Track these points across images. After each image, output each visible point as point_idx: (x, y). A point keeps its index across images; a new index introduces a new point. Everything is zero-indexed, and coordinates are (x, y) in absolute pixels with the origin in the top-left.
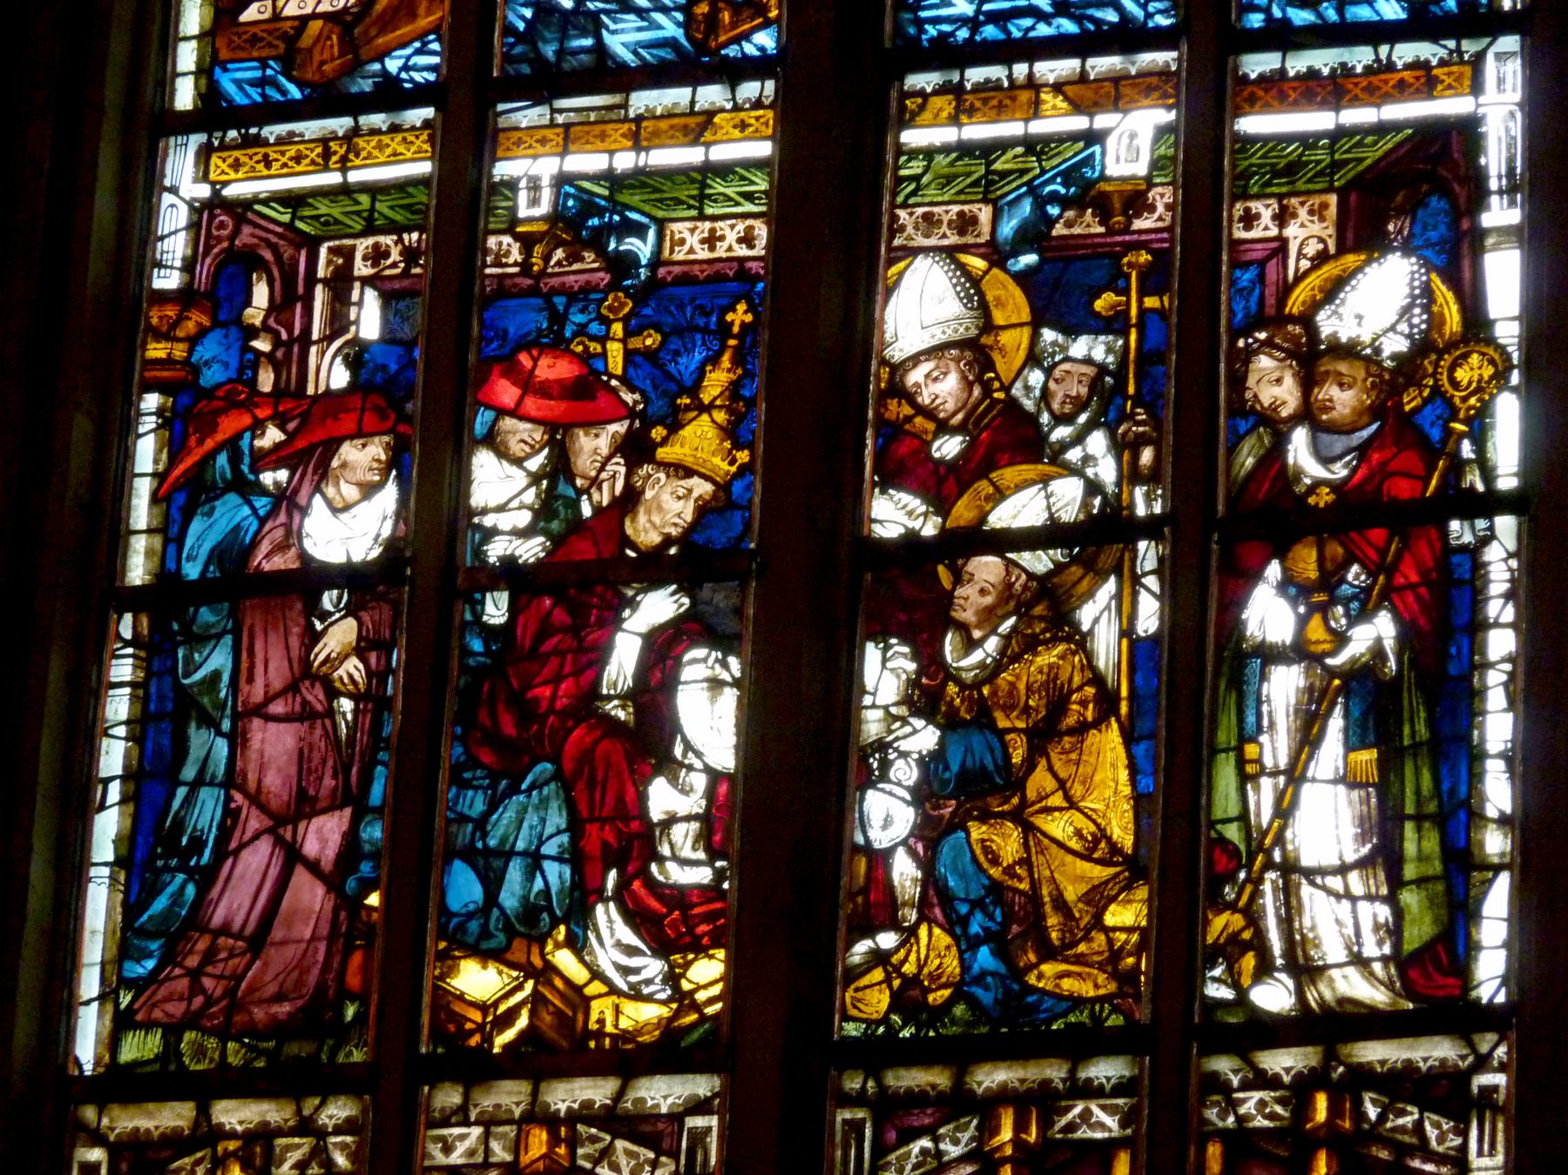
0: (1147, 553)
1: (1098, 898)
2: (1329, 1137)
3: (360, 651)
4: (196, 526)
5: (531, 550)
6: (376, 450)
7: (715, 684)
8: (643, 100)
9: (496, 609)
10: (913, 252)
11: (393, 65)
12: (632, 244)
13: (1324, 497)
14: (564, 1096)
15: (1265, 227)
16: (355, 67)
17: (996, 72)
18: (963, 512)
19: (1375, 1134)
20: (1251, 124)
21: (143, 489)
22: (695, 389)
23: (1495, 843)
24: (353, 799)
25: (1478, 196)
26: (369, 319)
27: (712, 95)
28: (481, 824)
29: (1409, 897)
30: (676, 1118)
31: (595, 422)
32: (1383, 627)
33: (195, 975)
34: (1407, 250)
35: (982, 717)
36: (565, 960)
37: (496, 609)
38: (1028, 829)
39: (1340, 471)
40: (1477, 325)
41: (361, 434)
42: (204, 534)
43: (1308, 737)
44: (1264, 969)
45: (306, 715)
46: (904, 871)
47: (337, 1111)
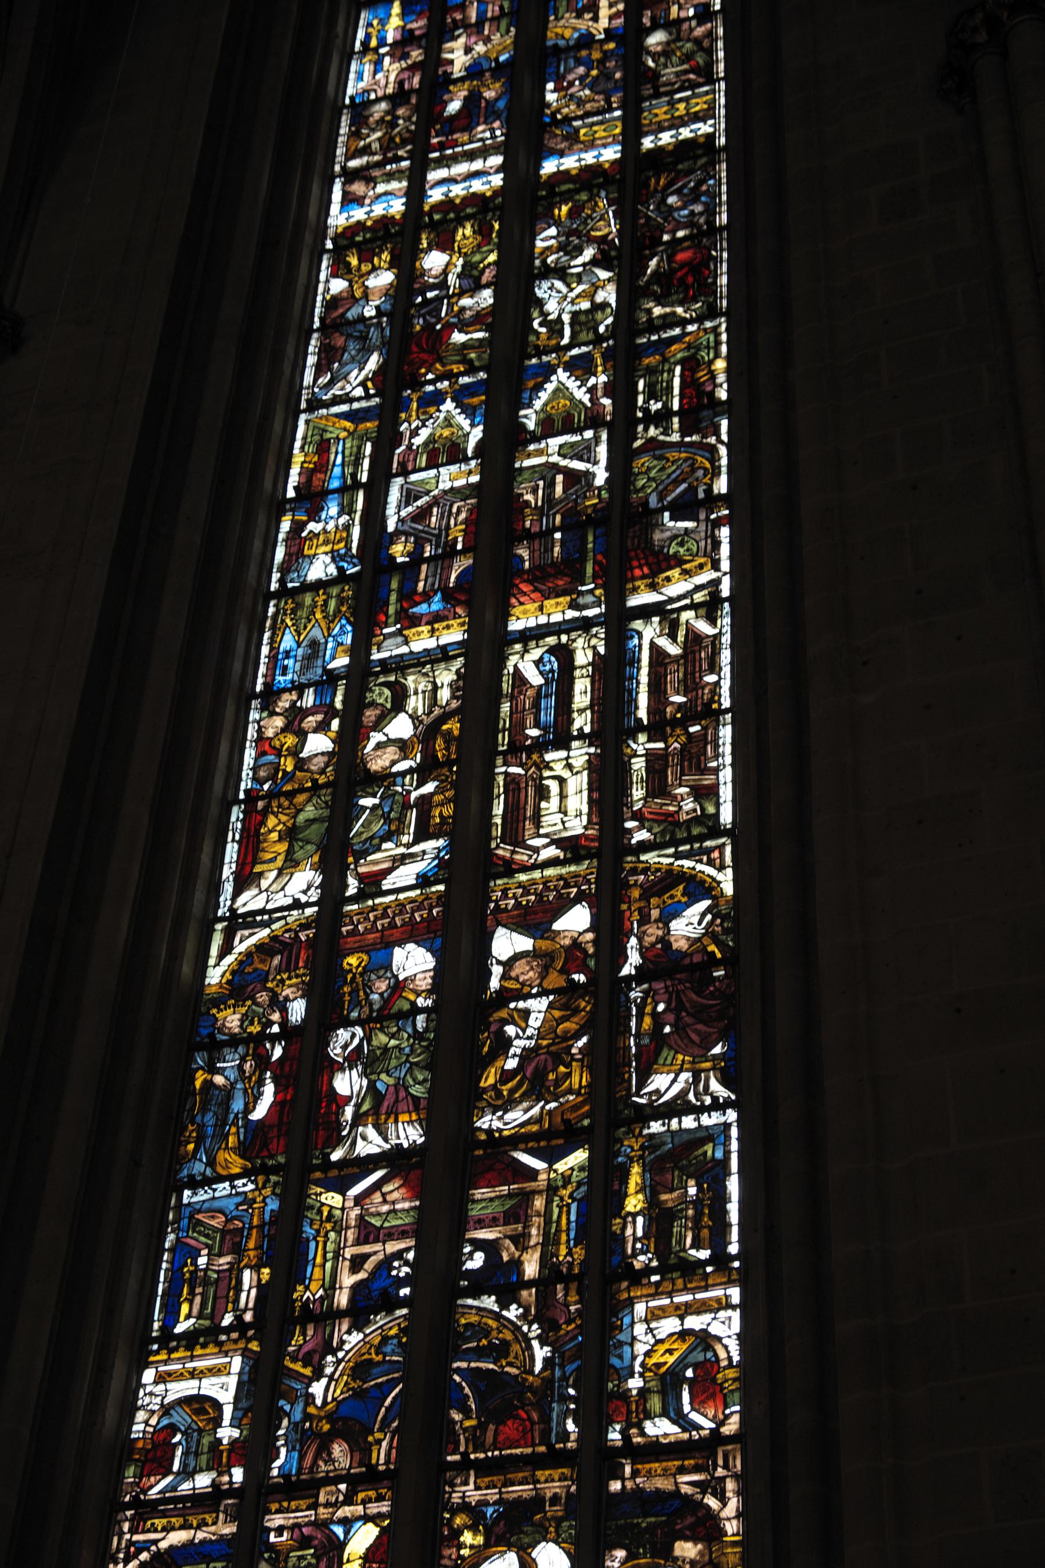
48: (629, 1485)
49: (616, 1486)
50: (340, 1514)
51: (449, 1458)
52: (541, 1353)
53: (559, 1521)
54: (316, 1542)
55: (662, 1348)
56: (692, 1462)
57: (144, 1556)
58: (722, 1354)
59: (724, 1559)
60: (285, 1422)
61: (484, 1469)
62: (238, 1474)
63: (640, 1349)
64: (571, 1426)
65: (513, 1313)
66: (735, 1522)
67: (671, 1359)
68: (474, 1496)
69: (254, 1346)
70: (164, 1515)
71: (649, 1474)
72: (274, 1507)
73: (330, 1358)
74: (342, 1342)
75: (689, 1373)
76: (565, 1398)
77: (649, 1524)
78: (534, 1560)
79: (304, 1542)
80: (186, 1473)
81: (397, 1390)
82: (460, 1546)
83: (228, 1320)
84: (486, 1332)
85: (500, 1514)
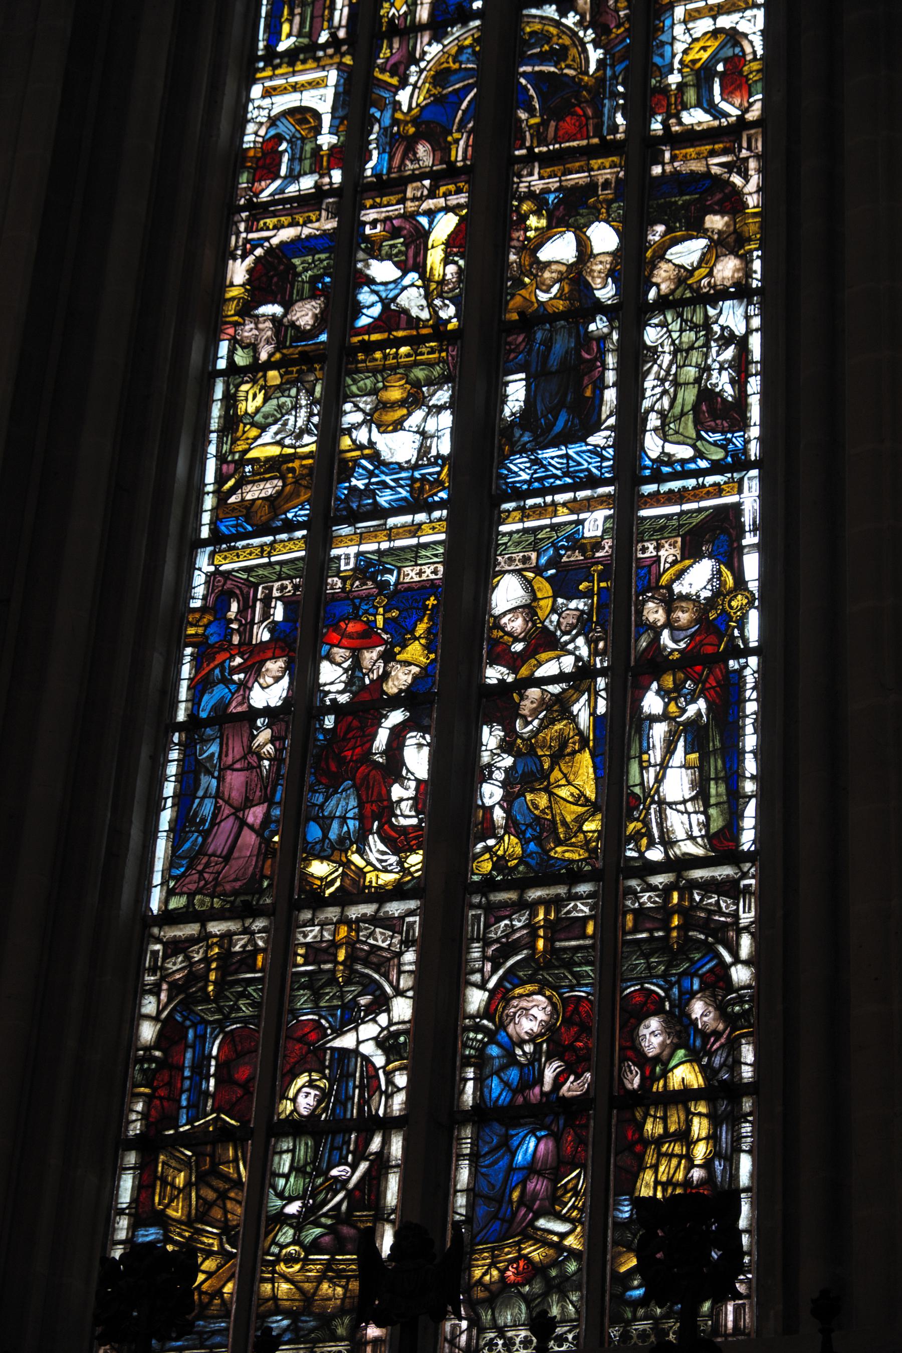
0: (601, 682)
1: (580, 820)
2: (679, 909)
3: (272, 741)
4: (206, 698)
5: (343, 699)
6: (281, 663)
7: (420, 746)
8: (392, 521)
9: (329, 722)
10: (504, 572)
11: (290, 515)
12: (387, 577)
13: (676, 655)
14: (354, 912)
15: (651, 552)
16: (275, 517)
17: (539, 500)
18: (524, 672)
19: (698, 907)
20: (644, 513)
21: (184, 685)
22: (412, 631)
23: (749, 787)
24: (269, 800)
25: (741, 534)
26: (279, 614)
27: (421, 517)
28: (322, 807)
29: (713, 811)
30: (402, 918)
31: (370, 647)
32: (702, 704)
33: (201, 873)
34: (710, 558)
35: (532, 750)
36: (356, 859)
37: (329, 722)
38: (551, 794)
39: (682, 645)
40: (740, 582)
41: (275, 657)
42: (208, 701)
43: (669, 750)
44: (651, 844)
45: (249, 768)
46: (499, 815)
47: (259, 924)
48: (668, 168)
49: (657, 170)
50: (425, 206)
51: (517, 153)
52: (595, 55)
53: (609, 203)
54: (405, 232)
55: (697, 46)
56: (721, 146)
57: (259, 252)
58: (748, 49)
59: (746, 228)
60: (376, 128)
61: (546, 160)
62: (337, 176)
63: (679, 47)
64: (620, 119)
65: (571, 20)
66: (755, 196)
67: (705, 56)
68: (538, 185)
69: (348, 60)
70: (274, 214)
71: (685, 159)
72: (369, 203)
73: (413, 68)
74: (424, 53)
75: (720, 67)
76: (616, 95)
77: (684, 201)
78: (588, 238)
79: (395, 233)
80: (293, 177)
81: (472, 94)
82: (527, 229)
83: (324, 37)
84: (547, 38)
85: (560, 200)
